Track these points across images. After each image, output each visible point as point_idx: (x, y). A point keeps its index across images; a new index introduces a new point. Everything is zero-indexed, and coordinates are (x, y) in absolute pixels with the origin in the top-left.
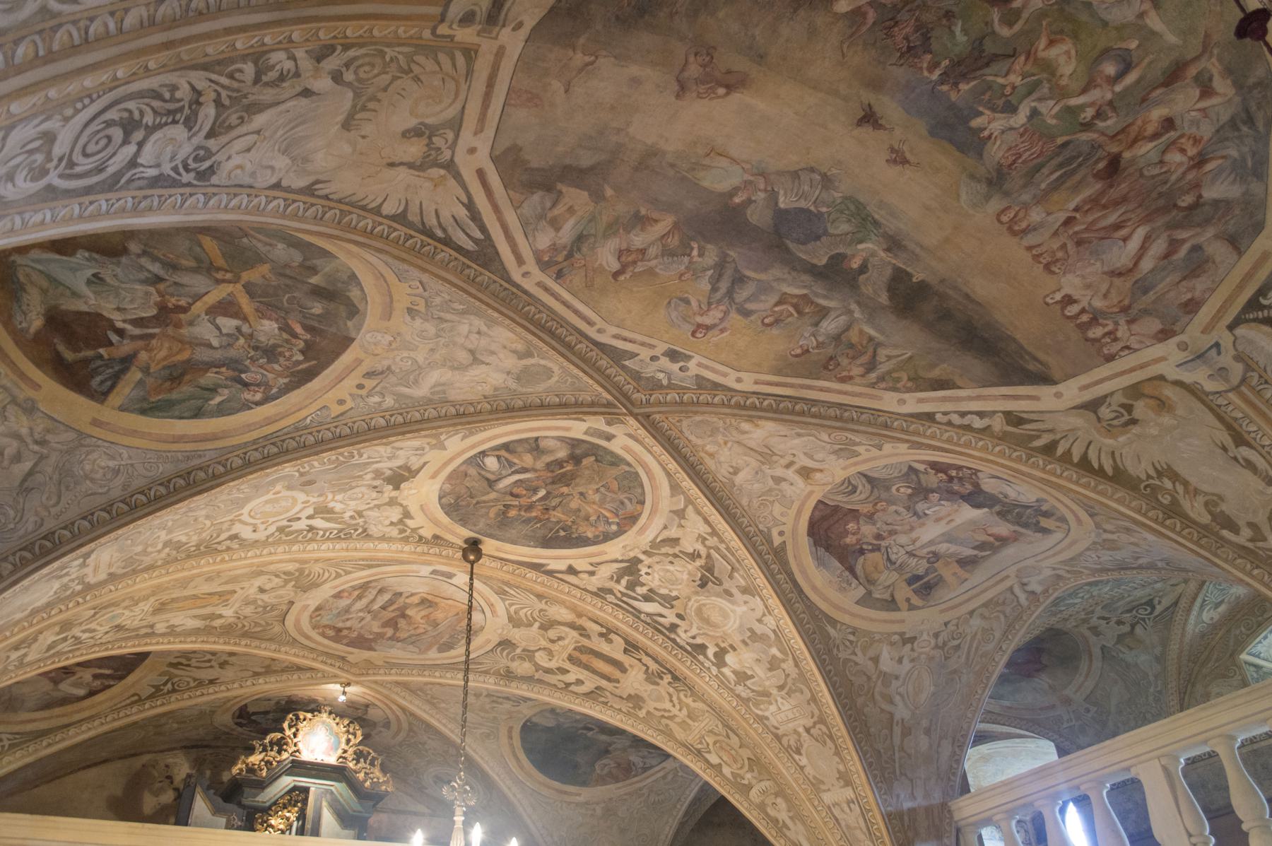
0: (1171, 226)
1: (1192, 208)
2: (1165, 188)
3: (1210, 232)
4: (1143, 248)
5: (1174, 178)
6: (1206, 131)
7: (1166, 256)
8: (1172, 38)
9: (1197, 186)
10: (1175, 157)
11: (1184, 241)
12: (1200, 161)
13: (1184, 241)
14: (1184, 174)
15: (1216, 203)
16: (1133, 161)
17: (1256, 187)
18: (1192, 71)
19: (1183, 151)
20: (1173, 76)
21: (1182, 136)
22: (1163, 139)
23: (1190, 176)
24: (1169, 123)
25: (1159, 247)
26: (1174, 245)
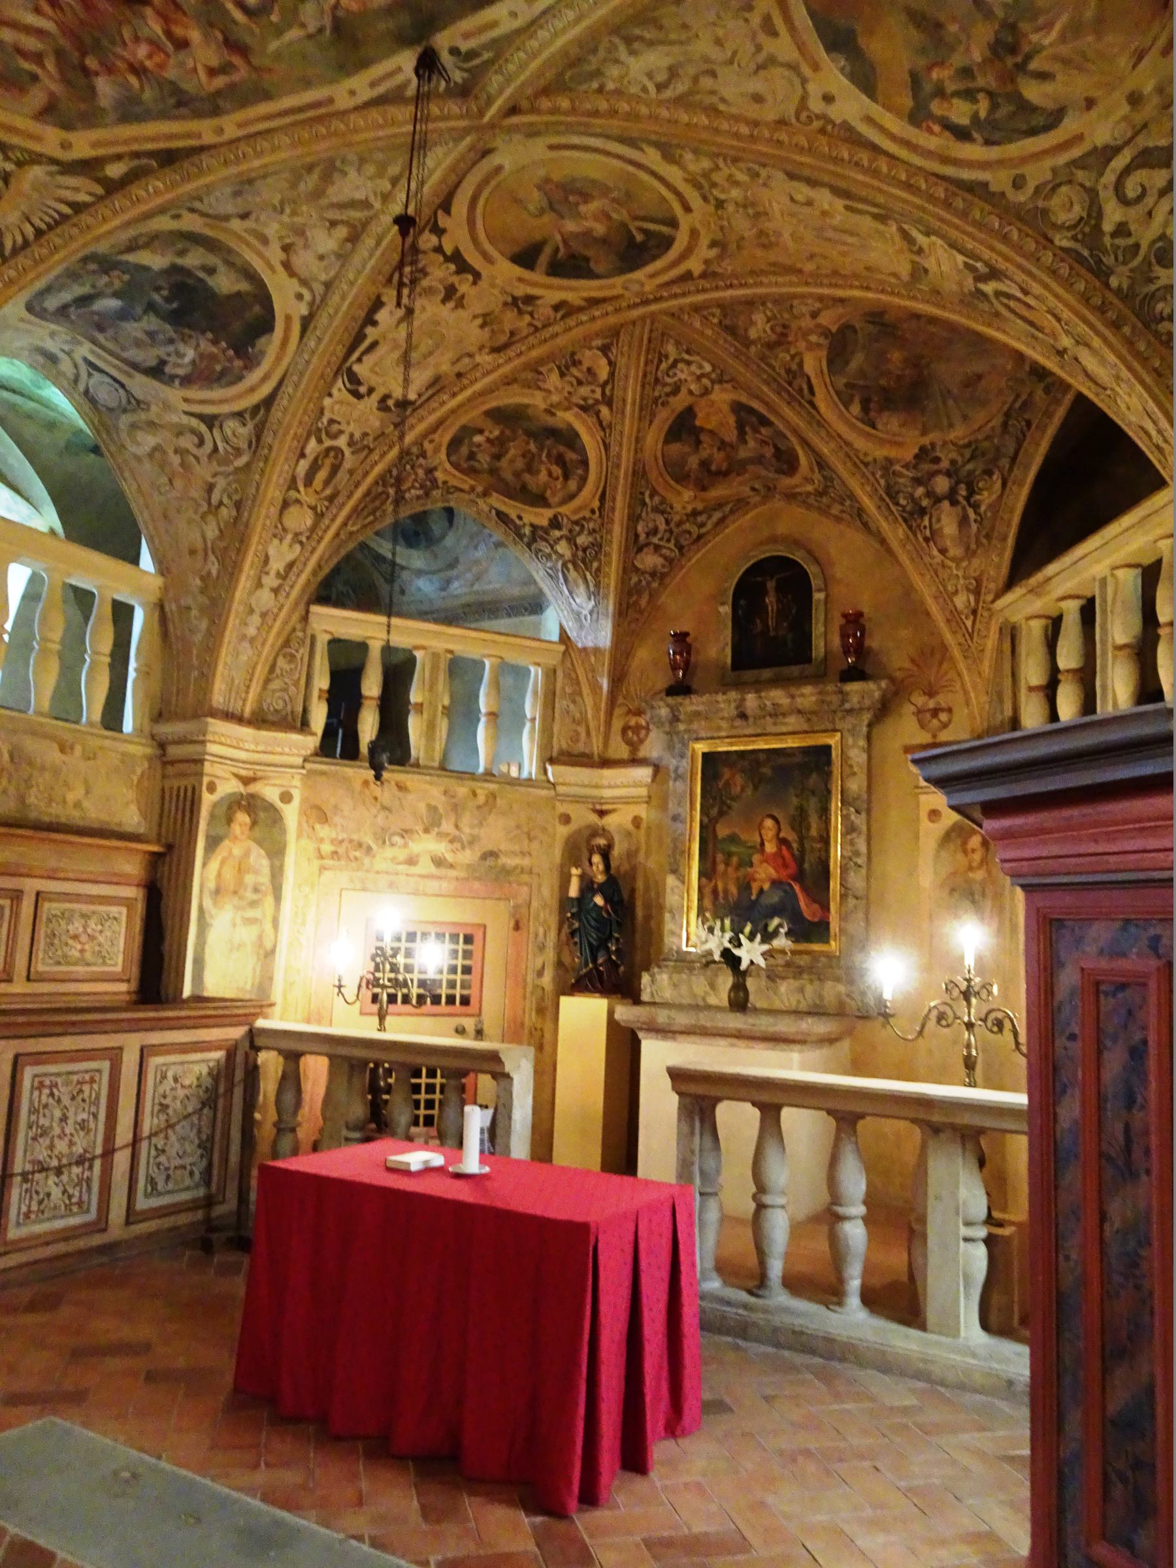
0: (59, 54)
1: (86, 72)
2: (105, 43)
3: (55, 87)
4: (28, 30)
5: (119, 50)
6: (171, 73)
7: (20, 52)
8: (274, 45)
9: (110, 70)
10: (142, 51)
11: (43, 66)
12: (138, 70)
13: (43, 66)
14: (122, 58)
15: (93, 90)
16: (143, 17)
17: (112, 116)
18: (237, 60)
19: (150, 56)
20: (234, 45)
21: (167, 55)
22: (168, 44)
23: (119, 64)
24: (182, 44)
25: (31, 43)
26: (38, 58)
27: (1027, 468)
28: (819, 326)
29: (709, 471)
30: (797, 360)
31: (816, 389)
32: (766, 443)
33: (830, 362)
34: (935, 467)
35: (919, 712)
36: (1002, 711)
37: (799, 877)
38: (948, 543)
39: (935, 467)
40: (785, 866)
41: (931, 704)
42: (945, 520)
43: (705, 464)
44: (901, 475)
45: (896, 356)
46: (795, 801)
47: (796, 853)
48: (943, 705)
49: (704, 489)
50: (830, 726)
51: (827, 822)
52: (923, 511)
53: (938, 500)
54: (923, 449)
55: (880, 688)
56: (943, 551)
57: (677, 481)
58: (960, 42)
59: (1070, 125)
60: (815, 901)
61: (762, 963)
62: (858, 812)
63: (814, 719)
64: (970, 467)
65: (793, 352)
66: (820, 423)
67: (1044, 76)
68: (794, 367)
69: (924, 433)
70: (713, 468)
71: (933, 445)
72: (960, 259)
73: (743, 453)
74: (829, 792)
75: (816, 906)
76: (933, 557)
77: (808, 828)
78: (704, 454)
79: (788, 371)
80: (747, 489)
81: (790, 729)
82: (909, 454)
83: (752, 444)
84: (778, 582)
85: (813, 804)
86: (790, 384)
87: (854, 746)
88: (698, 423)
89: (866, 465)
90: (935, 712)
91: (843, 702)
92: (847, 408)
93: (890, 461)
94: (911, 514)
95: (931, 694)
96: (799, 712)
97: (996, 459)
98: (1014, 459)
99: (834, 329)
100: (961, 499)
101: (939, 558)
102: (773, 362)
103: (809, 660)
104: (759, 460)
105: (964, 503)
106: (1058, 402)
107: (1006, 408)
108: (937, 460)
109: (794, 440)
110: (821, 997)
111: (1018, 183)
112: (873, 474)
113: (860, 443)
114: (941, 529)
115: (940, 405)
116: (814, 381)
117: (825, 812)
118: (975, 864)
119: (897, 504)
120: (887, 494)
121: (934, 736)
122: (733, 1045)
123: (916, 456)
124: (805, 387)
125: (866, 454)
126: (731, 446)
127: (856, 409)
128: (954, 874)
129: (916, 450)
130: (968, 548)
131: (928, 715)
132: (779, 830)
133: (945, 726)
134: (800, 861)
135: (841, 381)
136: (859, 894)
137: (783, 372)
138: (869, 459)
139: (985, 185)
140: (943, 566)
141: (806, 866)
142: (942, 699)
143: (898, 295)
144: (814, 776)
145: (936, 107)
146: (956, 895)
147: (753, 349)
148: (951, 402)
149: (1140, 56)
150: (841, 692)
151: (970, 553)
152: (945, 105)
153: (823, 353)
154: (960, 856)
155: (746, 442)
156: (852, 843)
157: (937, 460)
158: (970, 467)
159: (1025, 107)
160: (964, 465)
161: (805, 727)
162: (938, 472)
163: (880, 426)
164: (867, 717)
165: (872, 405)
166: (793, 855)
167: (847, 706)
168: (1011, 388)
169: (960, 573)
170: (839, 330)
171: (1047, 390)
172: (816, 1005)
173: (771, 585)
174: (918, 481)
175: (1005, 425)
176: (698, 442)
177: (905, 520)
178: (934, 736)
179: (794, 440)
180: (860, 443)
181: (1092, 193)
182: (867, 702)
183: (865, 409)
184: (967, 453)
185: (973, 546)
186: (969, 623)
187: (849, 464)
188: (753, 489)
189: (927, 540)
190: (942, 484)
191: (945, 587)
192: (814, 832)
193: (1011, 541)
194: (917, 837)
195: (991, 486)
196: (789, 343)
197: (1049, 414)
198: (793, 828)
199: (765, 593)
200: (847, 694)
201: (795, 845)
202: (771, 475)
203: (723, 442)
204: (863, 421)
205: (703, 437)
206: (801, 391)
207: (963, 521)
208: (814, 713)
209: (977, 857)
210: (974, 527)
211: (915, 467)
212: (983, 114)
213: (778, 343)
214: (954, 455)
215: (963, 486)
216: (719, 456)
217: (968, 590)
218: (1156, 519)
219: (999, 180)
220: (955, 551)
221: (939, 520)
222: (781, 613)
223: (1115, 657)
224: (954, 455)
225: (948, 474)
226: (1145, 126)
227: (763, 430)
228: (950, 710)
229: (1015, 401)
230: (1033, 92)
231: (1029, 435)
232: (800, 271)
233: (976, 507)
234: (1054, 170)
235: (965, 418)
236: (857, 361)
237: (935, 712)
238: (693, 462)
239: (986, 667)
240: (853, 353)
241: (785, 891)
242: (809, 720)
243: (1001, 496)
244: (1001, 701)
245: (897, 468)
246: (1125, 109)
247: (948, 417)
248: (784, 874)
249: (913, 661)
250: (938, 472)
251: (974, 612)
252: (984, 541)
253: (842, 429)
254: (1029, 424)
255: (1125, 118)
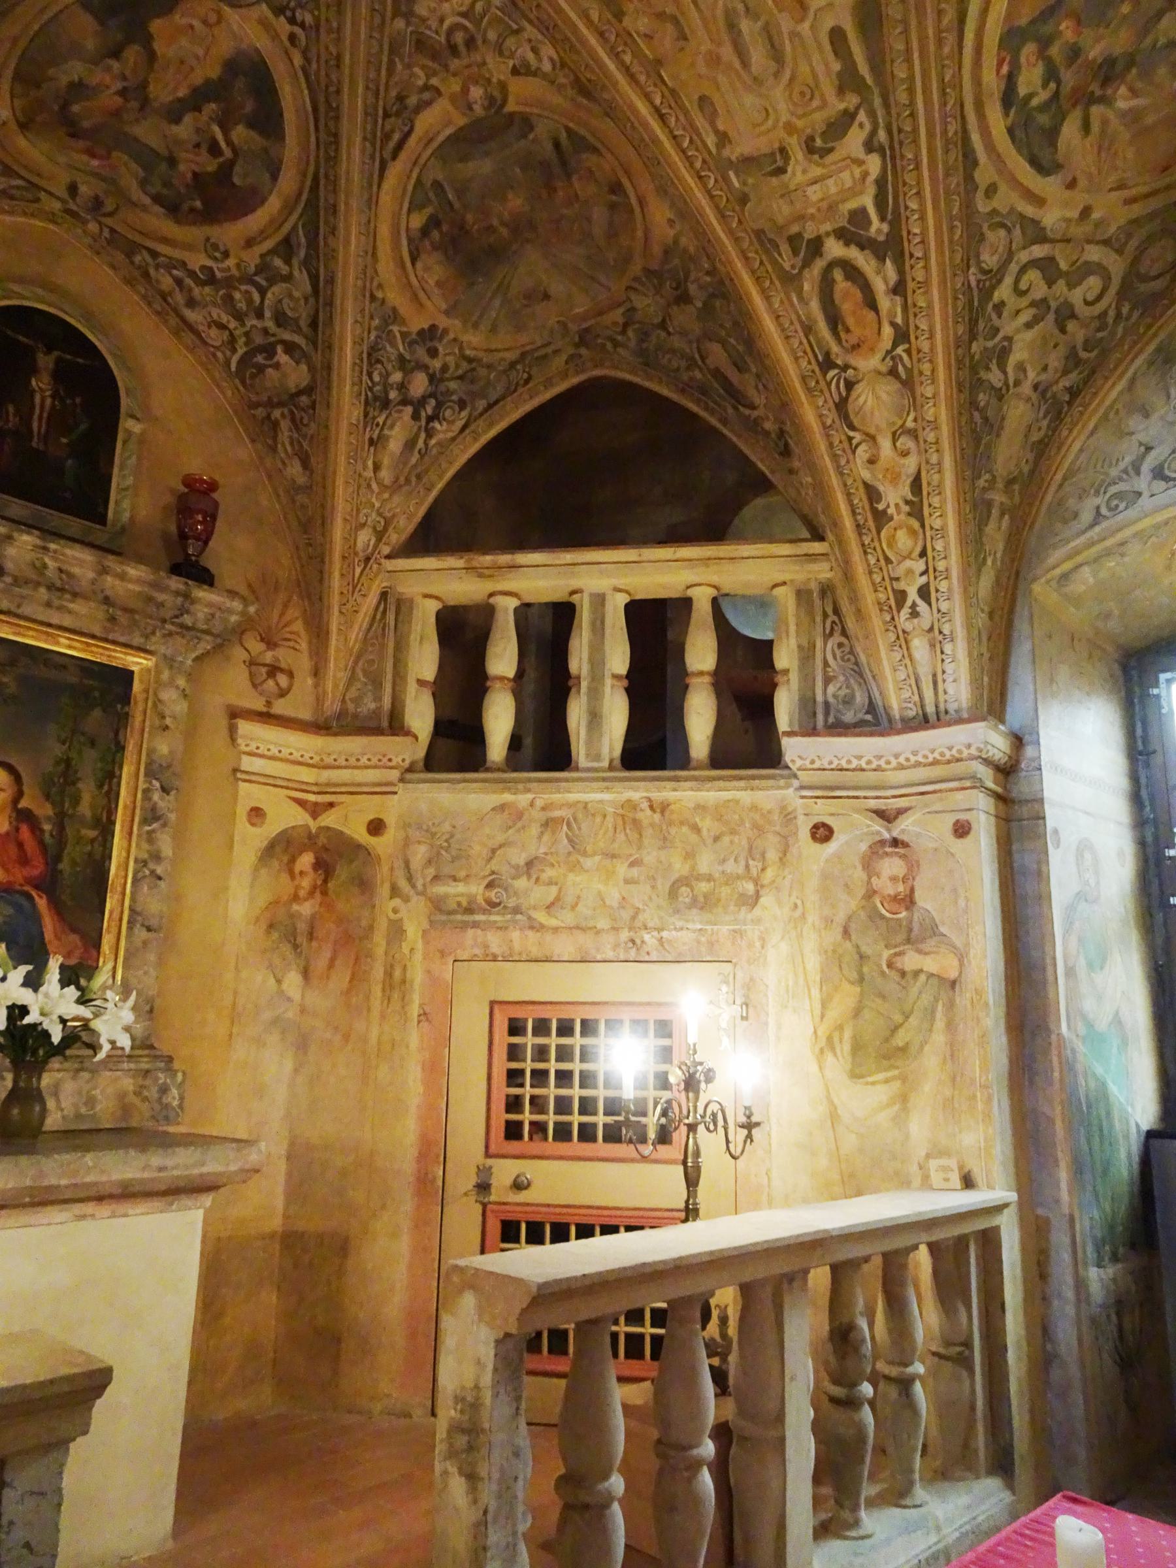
27: (491, 425)
28: (503, 86)
29: (65, 106)
30: (426, 96)
31: (403, 155)
32: (214, 150)
33: (453, 139)
34: (427, 359)
35: (252, 663)
36: (378, 699)
37: (49, 884)
38: (386, 461)
39: (427, 359)
40: (24, 861)
41: (268, 657)
42: (397, 429)
43: (78, 89)
44: (393, 344)
45: (516, 202)
46: (58, 750)
47: (47, 838)
48: (283, 665)
49: (23, 126)
50: (137, 640)
51: (112, 796)
52: (386, 404)
53: (405, 402)
54: (433, 327)
55: (243, 613)
56: (377, 467)
57: (18, 77)
58: (1107, 26)
59: (1049, 186)
60: (74, 930)
61: (125, 1042)
62: (165, 790)
63: (123, 619)
64: (453, 385)
65: (434, 81)
66: (372, 202)
67: (1086, 127)
68: (412, 101)
69: (447, 313)
70: (75, 108)
71: (445, 331)
72: (867, 201)
73: (148, 132)
74: (121, 748)
75: (74, 938)
76: (365, 468)
77: (76, 801)
78: (97, 77)
79: (401, 98)
80: (65, 178)
81: (67, 621)
82: (417, 324)
83: (184, 130)
84: (58, 361)
85: (88, 764)
86: (386, 115)
87: (171, 683)
88: (156, 26)
89: (373, 298)
90: (273, 670)
91: (183, 611)
92: (409, 211)
93: (394, 316)
94: (376, 398)
95: (271, 644)
96: (107, 601)
97: (474, 396)
98: (490, 406)
99: (511, 107)
100: (423, 414)
101: (369, 473)
102: (399, 67)
103: (102, 520)
104: (147, 158)
105: (423, 422)
106: (565, 375)
107: (528, 348)
108: (433, 353)
109: (288, 181)
110: (91, 1101)
111: (991, 190)
112: (372, 318)
113: (386, 268)
114: (387, 438)
115: (489, 294)
116: (412, 141)
117: (109, 778)
118: (302, 893)
119: (371, 378)
120: (369, 355)
121: (269, 703)
122: (82, 1217)
123: (421, 333)
124: (396, 137)
125: (380, 286)
126: (145, 103)
127: (417, 221)
128: (276, 902)
129: (426, 326)
130: (397, 479)
131: (264, 670)
132: (19, 794)
133: (283, 693)
134: (53, 858)
135: (436, 173)
136: (153, 922)
137: (393, 93)
138: (379, 295)
139: (975, 163)
140: (369, 486)
141: (64, 866)
142: (283, 656)
143: (690, 161)
144: (97, 713)
145: (1029, 50)
146: (275, 935)
147: (400, 24)
148: (497, 303)
149: (1121, 186)
150: (186, 596)
151: (395, 487)
152: (1033, 59)
153: (461, 121)
154: (284, 877)
155: (177, 120)
156: (150, 838)
157: (433, 353)
158: (453, 385)
159: (1052, 135)
160: (449, 380)
161: (97, 630)
162: (425, 368)
163: (419, 265)
164: (206, 644)
165: (435, 235)
166: (41, 843)
167: (187, 620)
168: (552, 332)
169: (377, 505)
170: (511, 115)
171: (571, 357)
172: (78, 1116)
173: (46, 361)
174: (402, 363)
175: (513, 365)
176: (116, 53)
177: (367, 403)
178: (269, 703)
179: (288, 181)
180: (386, 268)
181: (1010, 254)
182: (217, 627)
183: (425, 232)
184: (465, 365)
185: (402, 479)
186: (358, 570)
187: (360, 283)
188: (73, 189)
189: (372, 442)
190: (419, 385)
191: (358, 510)
192: (85, 808)
193: (434, 493)
194: (230, 846)
195: (453, 422)
196: (446, 67)
197: (549, 383)
198: (47, 797)
199: (34, 370)
200: (193, 602)
201: (47, 827)
202: (136, 194)
203: (144, 85)
204: (410, 240)
205: (132, 53)
206: (387, 137)
207: (410, 445)
208: (125, 610)
209: (306, 883)
210: (414, 459)
211: (411, 344)
212: (1035, 102)
213: (435, 56)
214: (451, 360)
215: (433, 402)
216: (109, 99)
217: (374, 528)
218: (727, 566)
219: (985, 174)
220: (386, 475)
221: (392, 427)
222: (58, 421)
223: (613, 687)
224: (451, 360)
225: (432, 378)
226: (1068, 241)
227: (240, 133)
228: (291, 674)
229: (543, 346)
230: (1070, 131)
231: (520, 390)
232: (619, 15)
233: (430, 434)
234: (1012, 210)
235: (494, 329)
236: (482, 167)
237: (273, 670)
238: (75, 70)
239: (355, 634)
240: (487, 154)
241: (19, 908)
242: (112, 619)
243: (453, 439)
244: (377, 684)
245: (395, 329)
246: (1074, 214)
247: (481, 316)
248: (19, 875)
249: (250, 586)
250: (425, 368)
251: (368, 559)
252: (414, 479)
253: (384, 230)
254: (527, 382)
255: (1068, 221)
